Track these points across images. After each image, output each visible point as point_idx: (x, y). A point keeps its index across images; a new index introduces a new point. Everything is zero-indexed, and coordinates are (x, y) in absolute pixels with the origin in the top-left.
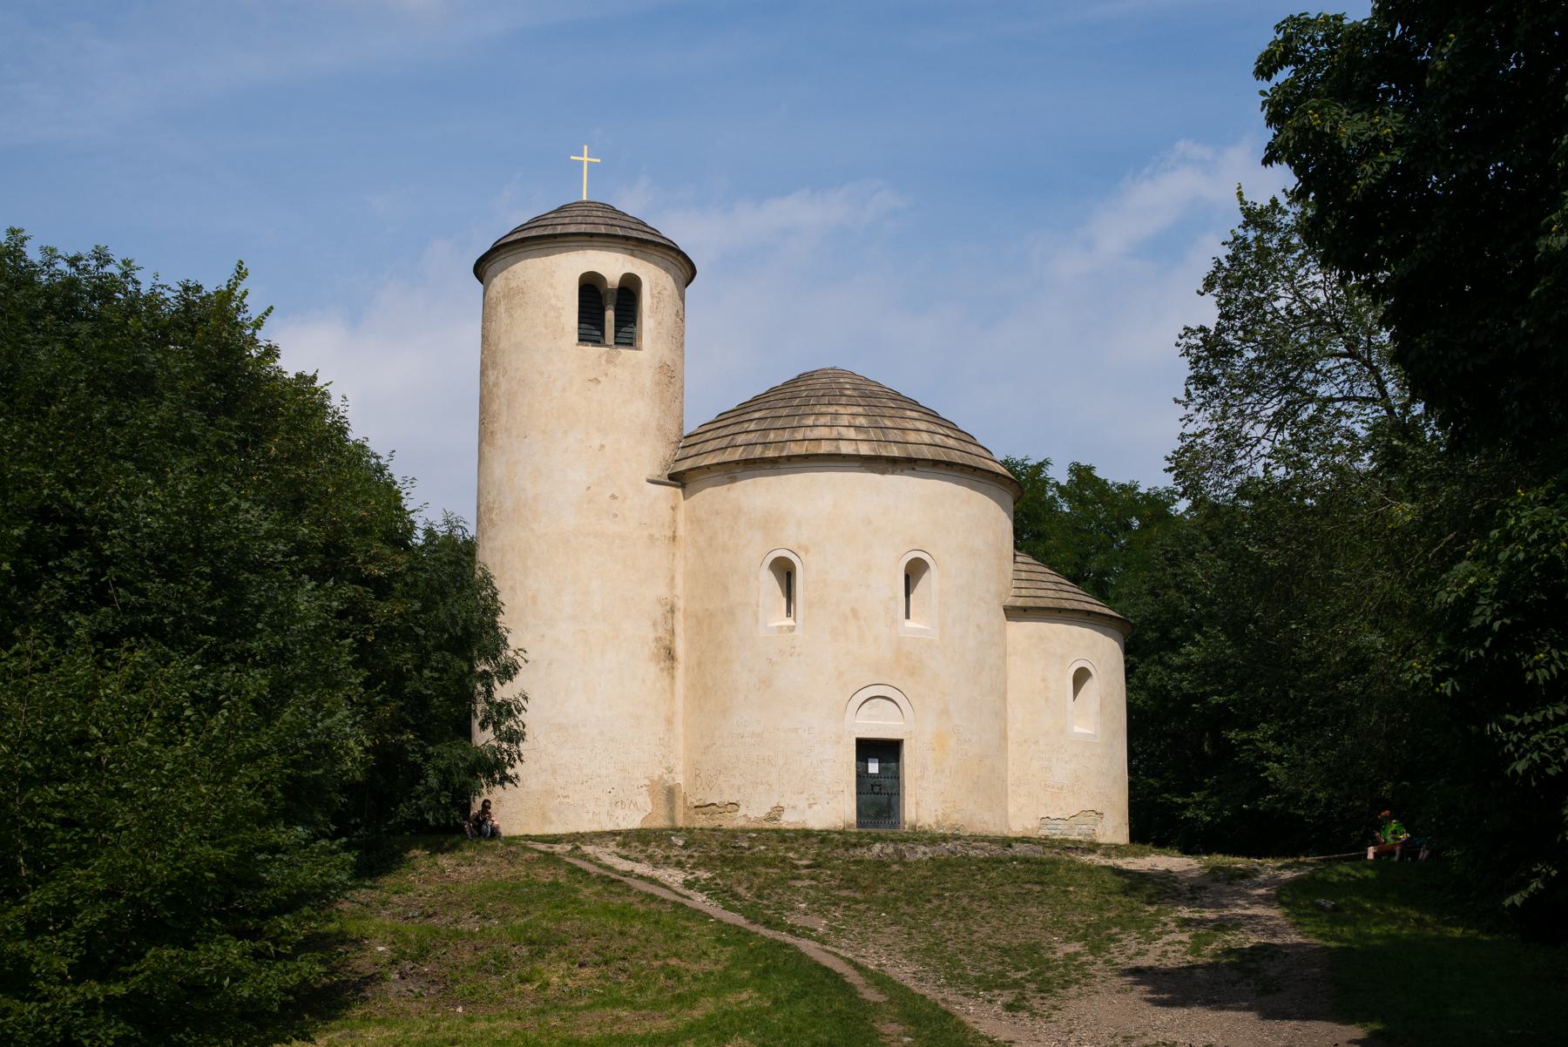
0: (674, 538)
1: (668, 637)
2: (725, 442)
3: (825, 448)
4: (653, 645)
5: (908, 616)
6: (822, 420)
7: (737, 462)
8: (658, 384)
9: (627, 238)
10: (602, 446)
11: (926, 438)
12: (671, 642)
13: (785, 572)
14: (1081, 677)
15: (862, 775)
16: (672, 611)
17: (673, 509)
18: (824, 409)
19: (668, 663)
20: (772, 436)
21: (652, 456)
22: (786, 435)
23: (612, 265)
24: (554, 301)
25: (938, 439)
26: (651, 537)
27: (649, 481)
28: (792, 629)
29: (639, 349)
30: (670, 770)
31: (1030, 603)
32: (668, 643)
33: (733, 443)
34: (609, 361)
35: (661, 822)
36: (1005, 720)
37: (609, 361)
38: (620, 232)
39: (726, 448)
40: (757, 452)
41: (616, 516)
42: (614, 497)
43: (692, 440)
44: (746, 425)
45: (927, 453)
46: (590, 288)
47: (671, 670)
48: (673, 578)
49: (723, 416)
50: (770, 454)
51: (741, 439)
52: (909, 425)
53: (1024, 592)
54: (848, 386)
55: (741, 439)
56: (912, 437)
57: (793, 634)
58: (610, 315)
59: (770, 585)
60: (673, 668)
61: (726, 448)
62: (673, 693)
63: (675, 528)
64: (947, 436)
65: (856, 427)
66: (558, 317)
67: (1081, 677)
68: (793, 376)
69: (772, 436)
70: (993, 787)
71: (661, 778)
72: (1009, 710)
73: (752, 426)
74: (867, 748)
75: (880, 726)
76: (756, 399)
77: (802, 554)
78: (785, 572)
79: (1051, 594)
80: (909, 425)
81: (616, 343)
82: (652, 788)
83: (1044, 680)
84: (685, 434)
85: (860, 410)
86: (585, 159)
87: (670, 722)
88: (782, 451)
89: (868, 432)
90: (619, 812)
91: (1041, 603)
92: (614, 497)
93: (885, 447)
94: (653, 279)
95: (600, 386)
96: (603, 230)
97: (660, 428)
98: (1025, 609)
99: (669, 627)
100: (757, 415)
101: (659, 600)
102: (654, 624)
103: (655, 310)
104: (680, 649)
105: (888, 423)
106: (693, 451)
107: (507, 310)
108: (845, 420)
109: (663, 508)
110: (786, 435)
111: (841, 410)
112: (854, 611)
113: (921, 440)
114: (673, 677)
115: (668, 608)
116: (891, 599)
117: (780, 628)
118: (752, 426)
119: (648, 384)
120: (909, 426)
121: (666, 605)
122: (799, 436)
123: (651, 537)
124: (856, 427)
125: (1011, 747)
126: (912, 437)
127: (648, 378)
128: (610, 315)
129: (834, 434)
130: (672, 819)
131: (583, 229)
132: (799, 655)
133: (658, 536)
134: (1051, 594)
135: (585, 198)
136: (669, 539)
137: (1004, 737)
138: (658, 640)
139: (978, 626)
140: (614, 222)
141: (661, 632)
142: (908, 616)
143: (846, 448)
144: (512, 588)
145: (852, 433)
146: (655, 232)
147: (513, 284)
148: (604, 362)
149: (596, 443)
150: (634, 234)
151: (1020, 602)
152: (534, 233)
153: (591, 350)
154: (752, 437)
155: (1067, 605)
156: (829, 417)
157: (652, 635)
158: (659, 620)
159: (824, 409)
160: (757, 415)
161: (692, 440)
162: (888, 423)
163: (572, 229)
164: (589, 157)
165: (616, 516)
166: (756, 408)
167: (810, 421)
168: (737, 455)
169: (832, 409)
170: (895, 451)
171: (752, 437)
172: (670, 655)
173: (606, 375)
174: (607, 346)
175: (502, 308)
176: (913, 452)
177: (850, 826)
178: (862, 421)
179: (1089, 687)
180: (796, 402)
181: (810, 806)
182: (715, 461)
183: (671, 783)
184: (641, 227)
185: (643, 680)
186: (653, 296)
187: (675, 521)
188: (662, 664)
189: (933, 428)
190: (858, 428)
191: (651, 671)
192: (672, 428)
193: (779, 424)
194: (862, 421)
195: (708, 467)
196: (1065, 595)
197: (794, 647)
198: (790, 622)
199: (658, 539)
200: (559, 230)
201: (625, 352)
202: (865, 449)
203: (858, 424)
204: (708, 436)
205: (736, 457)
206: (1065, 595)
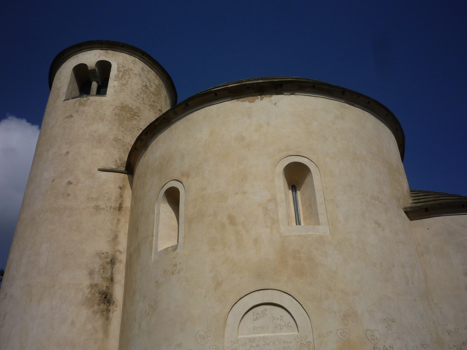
0: (120, 208)
1: (105, 284)
4: (87, 291)
5: (298, 222)
10: (68, 153)
16: (113, 262)
17: (121, 188)
19: (103, 306)
26: (97, 208)
32: (104, 289)
41: (69, 195)
48: (115, 238)
57: (175, 252)
60: (108, 310)
63: (122, 201)
77: (184, 180)
92: (70, 183)
95: (72, 119)
98: (427, 210)
99: (108, 275)
101: (99, 254)
102: (91, 274)
112: (232, 220)
114: (108, 319)
115: (108, 260)
116: (269, 201)
121: (106, 258)
132: (179, 272)
133: (103, 206)
136: (115, 209)
138: (93, 286)
139: (377, 223)
141: (97, 279)
142: (298, 222)
148: (77, 105)
149: (65, 151)
157: (86, 282)
158: (97, 270)
165: (69, 195)
173: (78, 111)
186: (119, 71)
187: (121, 196)
188: (96, 307)
197: (175, 265)
199: (103, 209)
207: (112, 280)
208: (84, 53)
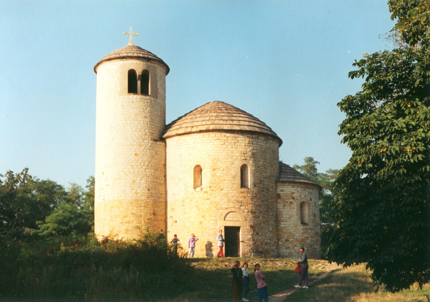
6: (212, 118)
11: (247, 123)
20: (195, 124)
25: (252, 124)
33: (182, 127)
39: (179, 128)
45: (247, 128)
46: (132, 74)
51: (184, 125)
52: (241, 119)
54: (221, 107)
55: (184, 125)
56: (242, 123)
58: (139, 83)
61: (179, 128)
64: (255, 123)
65: (223, 120)
80: (241, 119)
84: (167, 123)
85: (225, 114)
93: (233, 126)
105: (234, 118)
118: (188, 121)
124: (223, 120)
126: (242, 123)
128: (139, 83)
153: (133, 97)
162: (234, 118)
176: (242, 128)
184: (149, 54)
189: (249, 120)
193: (197, 120)
194: (226, 118)
203: (224, 119)
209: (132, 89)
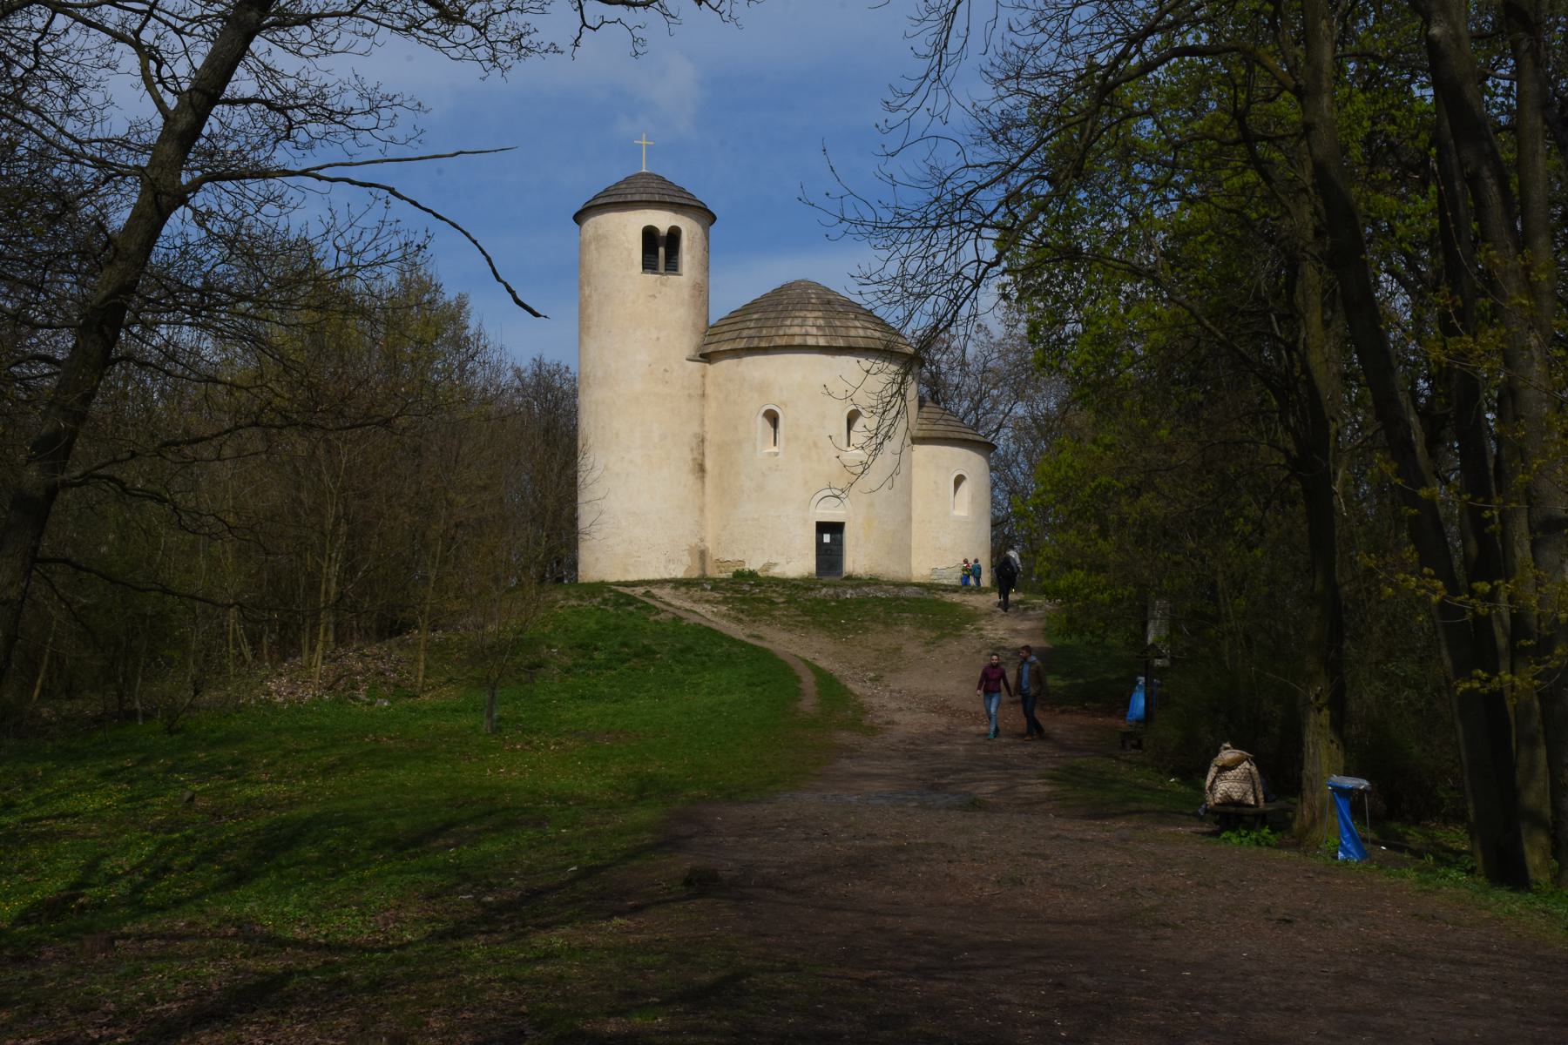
0: (703, 395)
1: (701, 457)
2: (735, 335)
3: (798, 341)
4: (691, 463)
6: (797, 321)
7: (742, 349)
8: (693, 297)
9: (672, 203)
10: (658, 339)
11: (861, 332)
12: (703, 460)
13: (772, 418)
14: (959, 480)
15: (819, 543)
16: (703, 441)
18: (797, 314)
20: (764, 332)
21: (686, 343)
22: (773, 332)
23: (663, 220)
24: (626, 245)
25: (869, 333)
27: (688, 360)
28: (776, 454)
29: (680, 275)
30: (702, 540)
31: (927, 434)
34: (662, 284)
35: (695, 574)
36: (911, 509)
37: (662, 284)
38: (668, 199)
40: (755, 343)
42: (666, 371)
43: (715, 330)
44: (748, 323)
45: (861, 343)
46: (649, 235)
47: (702, 478)
48: (703, 420)
49: (734, 314)
50: (763, 344)
51: (745, 333)
53: (924, 427)
55: (745, 333)
58: (662, 251)
59: (762, 424)
62: (703, 493)
66: (629, 255)
67: (959, 480)
68: (777, 285)
69: (764, 332)
70: (903, 549)
71: (696, 545)
72: (913, 503)
73: (752, 325)
74: (822, 527)
75: (830, 514)
76: (754, 303)
78: (772, 418)
79: (941, 427)
81: (666, 270)
82: (691, 551)
83: (935, 483)
84: (710, 324)
85: (820, 314)
86: (644, 142)
87: (702, 510)
88: (770, 342)
89: (824, 330)
90: (672, 566)
91: (934, 434)
92: (666, 371)
94: (689, 228)
96: (657, 198)
97: (694, 325)
100: (755, 316)
101: (695, 435)
102: (692, 450)
103: (690, 248)
104: (709, 464)
106: (716, 338)
107: (596, 249)
108: (810, 322)
109: (697, 376)
110: (773, 332)
111: (809, 315)
112: (815, 444)
113: (859, 332)
114: (703, 482)
117: (770, 453)
118: (752, 325)
119: (686, 297)
120: (850, 324)
122: (781, 333)
123: (690, 396)
125: (914, 526)
126: (853, 332)
127: (686, 294)
128: (662, 251)
129: (803, 331)
130: (703, 569)
131: (644, 197)
134: (941, 427)
135: (644, 170)
137: (910, 519)
138: (694, 459)
140: (664, 192)
141: (696, 455)
143: (811, 341)
144: (603, 427)
145: (814, 331)
146: (691, 197)
147: (600, 232)
150: (677, 200)
151: (920, 434)
152: (613, 200)
153: (651, 277)
154: (751, 332)
155: (951, 435)
156: (800, 320)
159: (797, 314)
160: (755, 316)
161: (715, 330)
162: (838, 323)
163: (637, 198)
164: (647, 145)
166: (753, 311)
167: (788, 322)
168: (742, 344)
169: (802, 314)
170: (841, 343)
171: (751, 332)
172: (701, 469)
174: (660, 274)
175: (593, 247)
176: (852, 342)
177: (812, 574)
178: (821, 322)
179: (964, 486)
180: (780, 307)
181: (788, 563)
182: (729, 348)
183: (703, 548)
185: (685, 486)
186: (689, 240)
190: (818, 327)
191: (690, 479)
192: (702, 324)
193: (769, 323)
194: (821, 322)
195: (725, 351)
196: (951, 428)
198: (775, 449)
200: (629, 198)
201: (672, 278)
202: (822, 342)
204: (725, 328)
205: (742, 346)
206: (951, 428)
207: (703, 454)
208: (653, 211)
209: (649, 264)
